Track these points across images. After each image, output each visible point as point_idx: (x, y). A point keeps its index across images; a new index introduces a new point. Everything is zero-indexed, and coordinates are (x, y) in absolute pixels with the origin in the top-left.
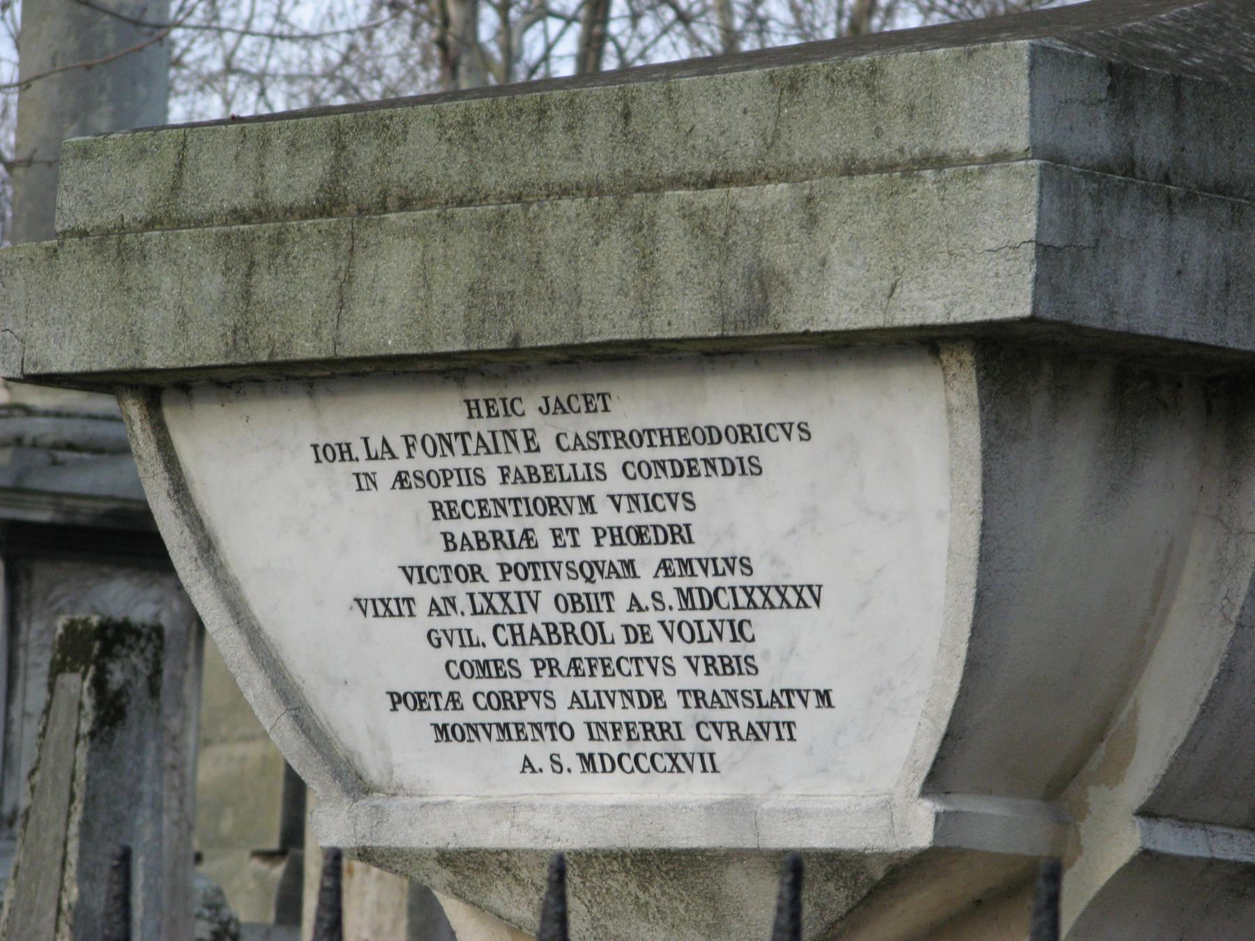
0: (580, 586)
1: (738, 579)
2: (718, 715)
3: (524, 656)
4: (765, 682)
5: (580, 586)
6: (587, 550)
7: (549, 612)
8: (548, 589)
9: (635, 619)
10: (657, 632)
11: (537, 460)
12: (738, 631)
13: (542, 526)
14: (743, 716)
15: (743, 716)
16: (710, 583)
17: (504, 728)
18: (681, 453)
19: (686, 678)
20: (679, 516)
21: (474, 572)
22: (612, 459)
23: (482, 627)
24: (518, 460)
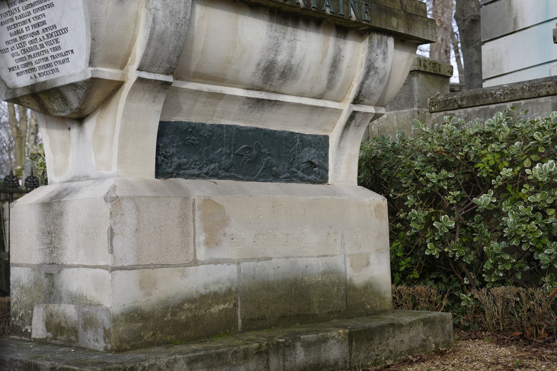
0: (32, 38)
1: (54, 30)
2: (57, 60)
3: (26, 55)
4: (63, 51)
5: (32, 38)
6: (31, 31)
7: (28, 46)
8: (28, 40)
9: (41, 43)
10: (45, 45)
11: (20, 14)
12: (57, 41)
13: (23, 27)
14: (61, 59)
15: (61, 59)
16: (50, 32)
17: (26, 71)
18: (41, 5)
19: (52, 53)
20: (43, 19)
21: (15, 40)
22: (31, 10)
23: (19, 51)
24: (17, 14)
